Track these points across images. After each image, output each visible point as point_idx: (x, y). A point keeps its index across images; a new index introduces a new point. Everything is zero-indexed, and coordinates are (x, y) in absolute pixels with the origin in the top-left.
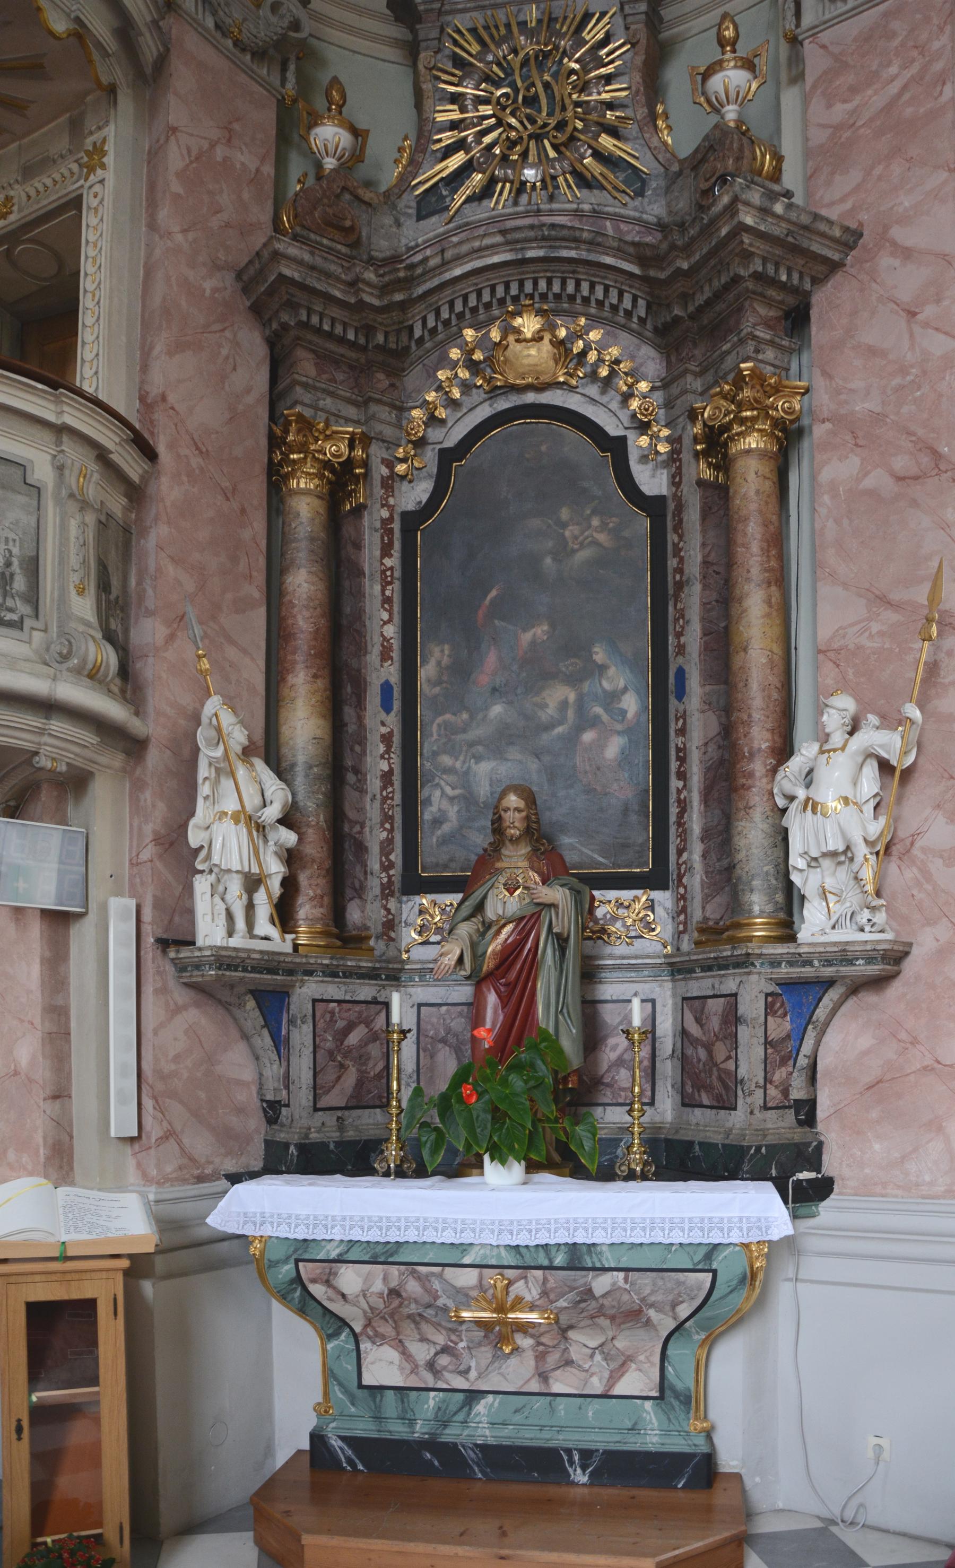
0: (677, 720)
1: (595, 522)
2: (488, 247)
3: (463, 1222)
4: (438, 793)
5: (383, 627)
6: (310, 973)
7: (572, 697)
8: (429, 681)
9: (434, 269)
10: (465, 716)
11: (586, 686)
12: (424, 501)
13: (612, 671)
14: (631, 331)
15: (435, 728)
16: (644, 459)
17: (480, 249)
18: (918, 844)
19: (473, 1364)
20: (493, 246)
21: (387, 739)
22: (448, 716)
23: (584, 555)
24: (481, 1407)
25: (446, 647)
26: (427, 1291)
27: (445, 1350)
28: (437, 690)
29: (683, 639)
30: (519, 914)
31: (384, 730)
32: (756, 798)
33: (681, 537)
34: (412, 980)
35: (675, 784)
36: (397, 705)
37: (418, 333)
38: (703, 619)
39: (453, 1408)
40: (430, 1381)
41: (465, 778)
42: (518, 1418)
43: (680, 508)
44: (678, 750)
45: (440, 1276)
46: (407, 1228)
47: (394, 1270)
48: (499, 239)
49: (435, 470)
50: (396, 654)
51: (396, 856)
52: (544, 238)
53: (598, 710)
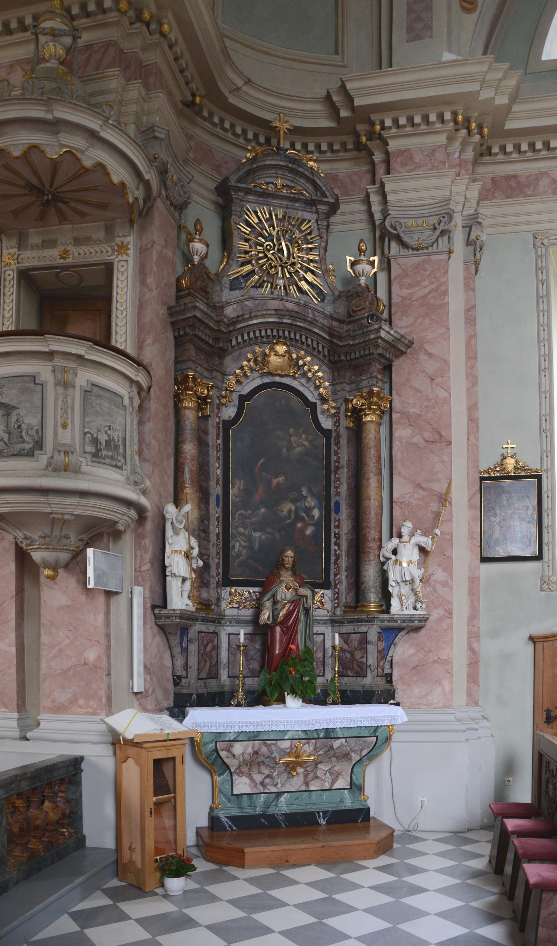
0: (335, 522)
1: (303, 436)
2: (268, 315)
3: (287, 722)
4: (238, 544)
5: (217, 471)
6: (197, 620)
7: (293, 508)
8: (234, 495)
9: (245, 319)
10: (250, 512)
11: (299, 504)
12: (232, 416)
13: (309, 499)
14: (319, 359)
15: (237, 515)
16: (323, 412)
17: (265, 315)
18: (432, 579)
19: (279, 781)
20: (271, 315)
21: (218, 519)
22: (242, 511)
23: (298, 449)
24: (282, 799)
25: (242, 481)
26: (269, 751)
27: (268, 776)
28: (238, 499)
29: (339, 490)
30: (292, 600)
31: (217, 515)
32: (372, 557)
33: (339, 448)
34: (226, 623)
35: (333, 547)
36: (221, 504)
37: (234, 343)
38: (347, 483)
39: (271, 800)
40: (261, 789)
41: (249, 539)
42: (296, 802)
43: (338, 436)
44: (335, 534)
45: (276, 744)
46: (265, 725)
47: (257, 743)
48: (273, 312)
49: (237, 404)
50: (221, 482)
51: (220, 570)
52: (292, 316)
53: (304, 515)
